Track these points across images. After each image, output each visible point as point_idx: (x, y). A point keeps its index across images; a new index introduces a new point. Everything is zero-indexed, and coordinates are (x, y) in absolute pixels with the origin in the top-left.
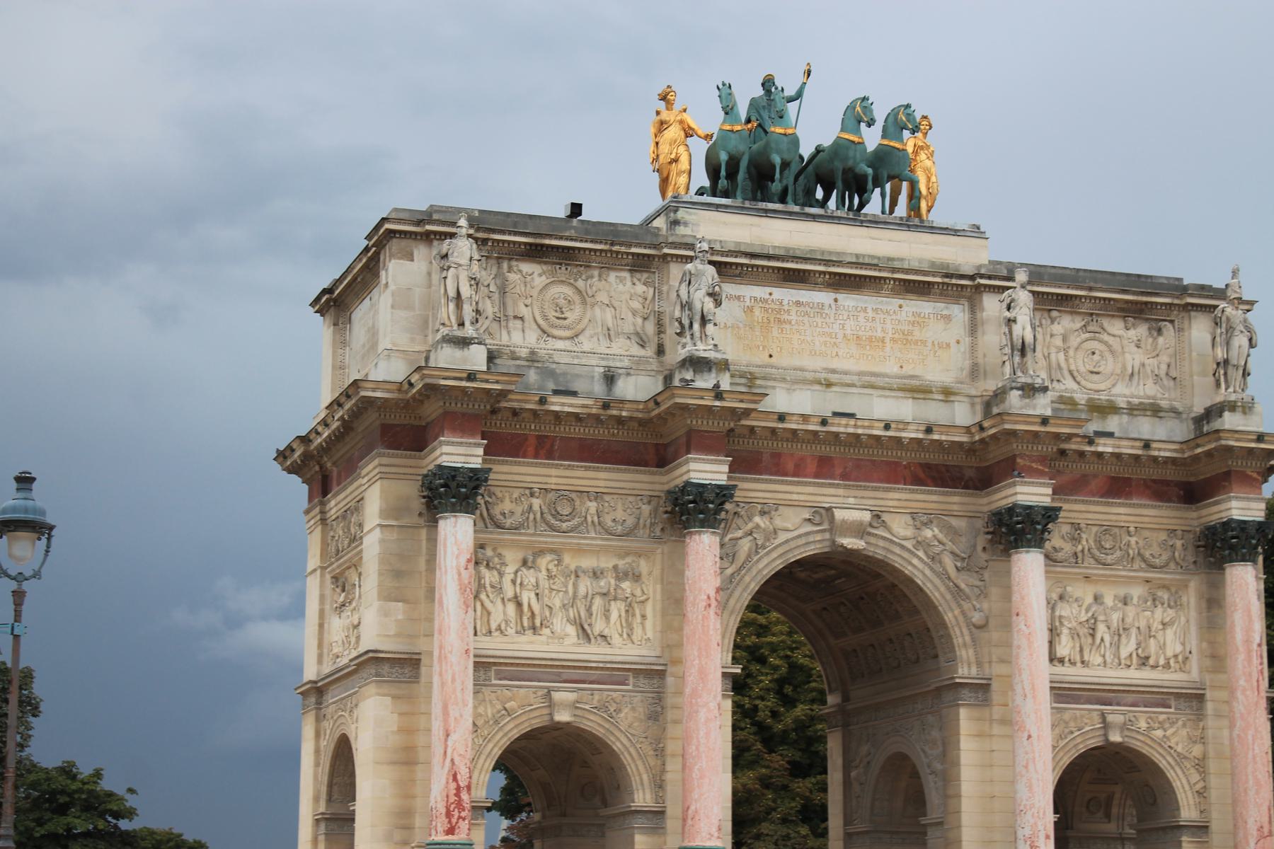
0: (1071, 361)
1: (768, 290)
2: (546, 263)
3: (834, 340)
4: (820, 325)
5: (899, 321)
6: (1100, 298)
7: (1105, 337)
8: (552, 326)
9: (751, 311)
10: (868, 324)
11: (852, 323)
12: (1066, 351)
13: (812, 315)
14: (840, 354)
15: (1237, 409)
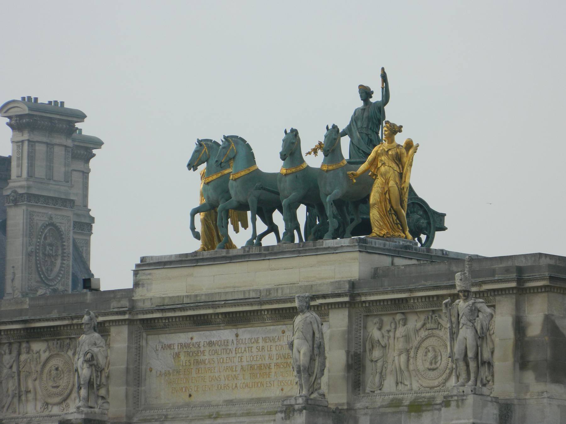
0: (411, 360)
1: (190, 335)
2: (47, 341)
3: (234, 373)
4: (225, 359)
5: (282, 346)
6: (425, 297)
7: (441, 333)
8: (50, 396)
9: (179, 357)
10: (259, 353)
11: (248, 354)
12: (408, 351)
13: (220, 353)
14: (238, 385)
15: (453, 404)
